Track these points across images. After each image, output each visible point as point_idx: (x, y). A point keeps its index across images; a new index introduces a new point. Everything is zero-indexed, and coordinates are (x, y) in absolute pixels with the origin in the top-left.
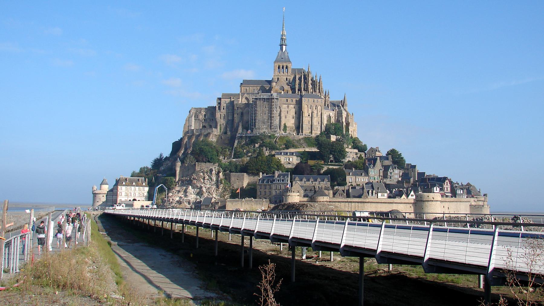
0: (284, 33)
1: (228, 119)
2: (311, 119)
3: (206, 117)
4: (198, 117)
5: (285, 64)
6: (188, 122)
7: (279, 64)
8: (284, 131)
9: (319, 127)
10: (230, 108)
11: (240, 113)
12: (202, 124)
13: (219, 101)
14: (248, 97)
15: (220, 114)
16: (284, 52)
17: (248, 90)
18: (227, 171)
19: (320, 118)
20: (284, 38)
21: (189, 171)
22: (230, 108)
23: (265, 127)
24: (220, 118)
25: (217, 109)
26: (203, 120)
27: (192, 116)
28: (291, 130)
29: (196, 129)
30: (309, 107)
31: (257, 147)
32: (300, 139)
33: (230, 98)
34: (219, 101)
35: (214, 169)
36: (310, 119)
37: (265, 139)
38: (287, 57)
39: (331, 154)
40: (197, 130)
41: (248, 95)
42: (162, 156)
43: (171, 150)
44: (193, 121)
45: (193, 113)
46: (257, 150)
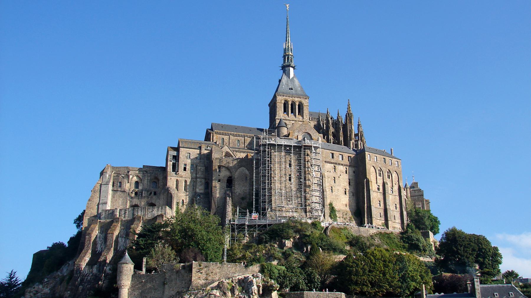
0: (290, 47)
1: (196, 193)
2: (382, 197)
3: (140, 188)
4: (120, 186)
5: (297, 100)
6: (98, 196)
7: (287, 98)
8: (331, 218)
9: (398, 215)
10: (199, 168)
11: (226, 179)
12: (131, 201)
13: (175, 153)
14: (231, 153)
15: (177, 181)
16: (293, 78)
17: (226, 141)
18: (286, 286)
19: (398, 198)
20: (290, 53)
21: (166, 286)
22: (199, 168)
23: (291, 206)
24: (177, 188)
25: (170, 168)
26: (132, 193)
27: (109, 182)
28: (345, 216)
29: (121, 210)
30: (378, 172)
31: (290, 248)
32: (371, 236)
33: (200, 148)
34: (175, 153)
35: (254, 280)
36: (381, 197)
37: (306, 229)
38: (299, 89)
39: (477, 262)
40: (123, 212)
41: (231, 149)
42: (13, 278)
43: (30, 271)
44: (109, 192)
45: (110, 176)
46: (293, 253)
